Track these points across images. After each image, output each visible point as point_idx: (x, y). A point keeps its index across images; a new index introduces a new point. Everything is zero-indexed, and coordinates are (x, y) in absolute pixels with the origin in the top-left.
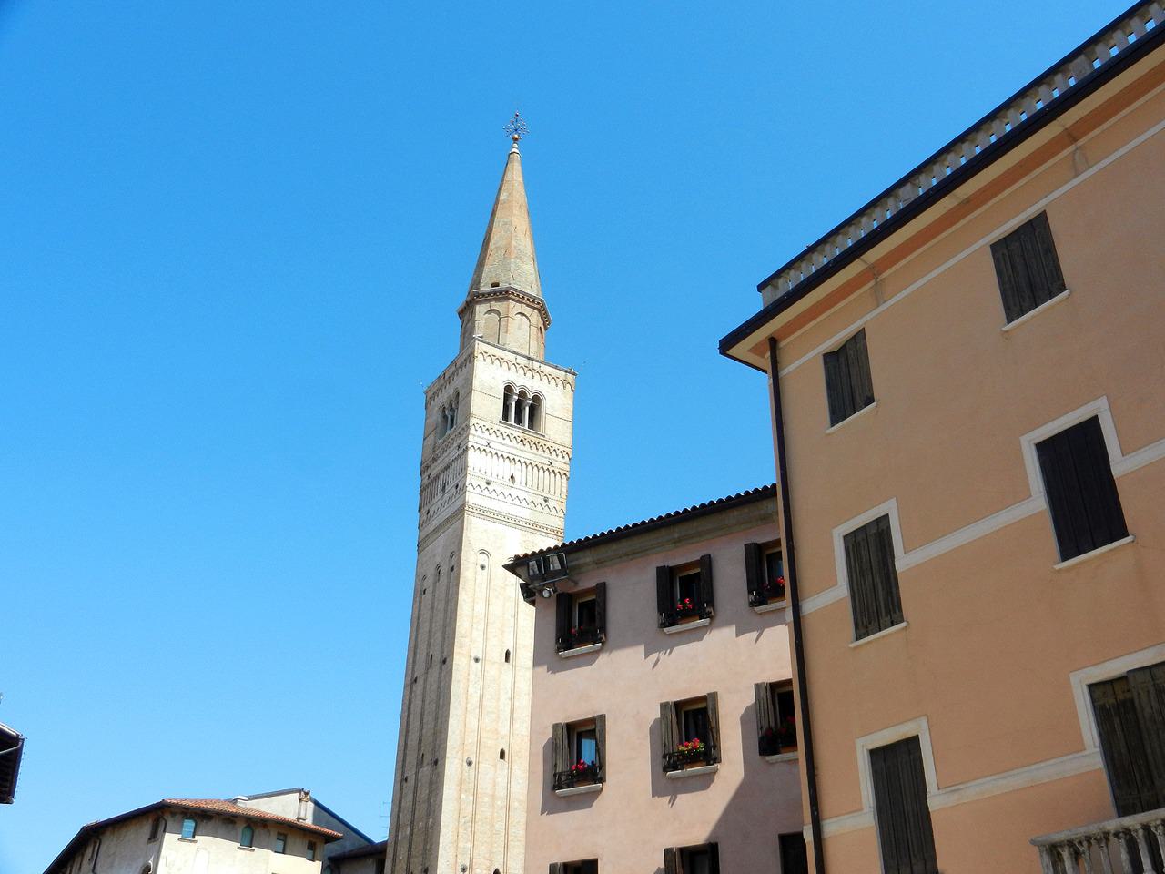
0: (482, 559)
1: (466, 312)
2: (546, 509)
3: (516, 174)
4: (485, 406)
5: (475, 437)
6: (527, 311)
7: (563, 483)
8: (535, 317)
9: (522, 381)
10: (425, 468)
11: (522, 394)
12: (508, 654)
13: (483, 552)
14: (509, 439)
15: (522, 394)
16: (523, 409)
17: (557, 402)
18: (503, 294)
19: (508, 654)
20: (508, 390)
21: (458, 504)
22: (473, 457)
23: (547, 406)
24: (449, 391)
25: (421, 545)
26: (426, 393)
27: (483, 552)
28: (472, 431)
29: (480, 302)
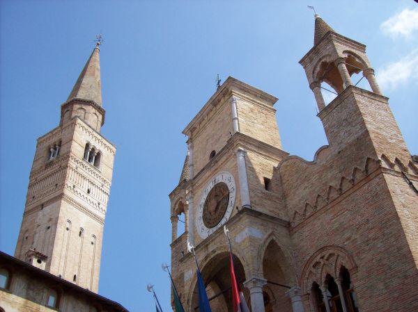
0: (68, 225)
1: (67, 108)
2: (98, 208)
3: (97, 56)
4: (77, 150)
5: (72, 163)
6: (98, 113)
7: (106, 198)
8: (100, 117)
9: (93, 143)
10: (33, 174)
11: (93, 149)
12: (75, 276)
13: (69, 221)
14: (86, 169)
15: (93, 149)
16: (93, 156)
17: (108, 157)
18: (89, 103)
19: (75, 276)
20: (88, 145)
21: (57, 194)
22: (70, 173)
23: (103, 159)
24: (55, 139)
25: (26, 213)
26: (38, 140)
27: (69, 221)
28: (70, 159)
29: (76, 103)
